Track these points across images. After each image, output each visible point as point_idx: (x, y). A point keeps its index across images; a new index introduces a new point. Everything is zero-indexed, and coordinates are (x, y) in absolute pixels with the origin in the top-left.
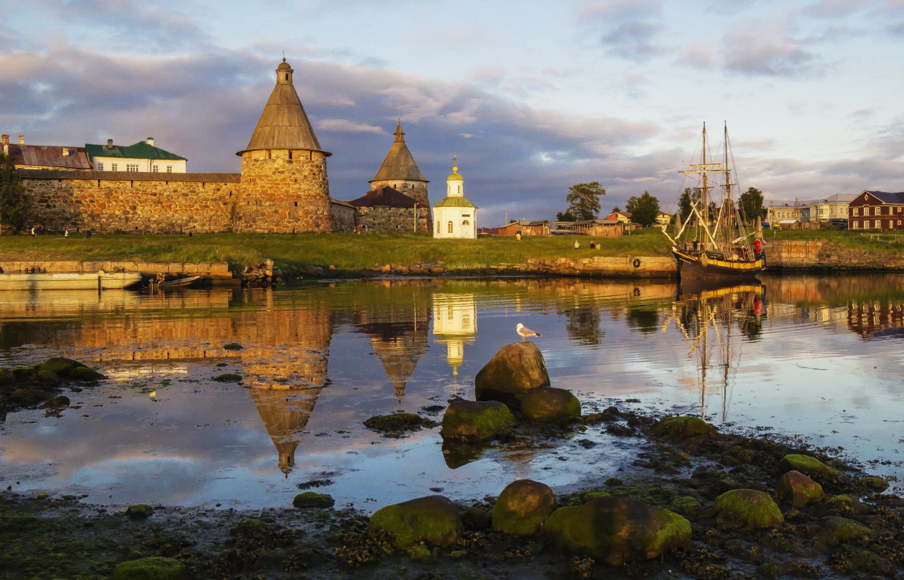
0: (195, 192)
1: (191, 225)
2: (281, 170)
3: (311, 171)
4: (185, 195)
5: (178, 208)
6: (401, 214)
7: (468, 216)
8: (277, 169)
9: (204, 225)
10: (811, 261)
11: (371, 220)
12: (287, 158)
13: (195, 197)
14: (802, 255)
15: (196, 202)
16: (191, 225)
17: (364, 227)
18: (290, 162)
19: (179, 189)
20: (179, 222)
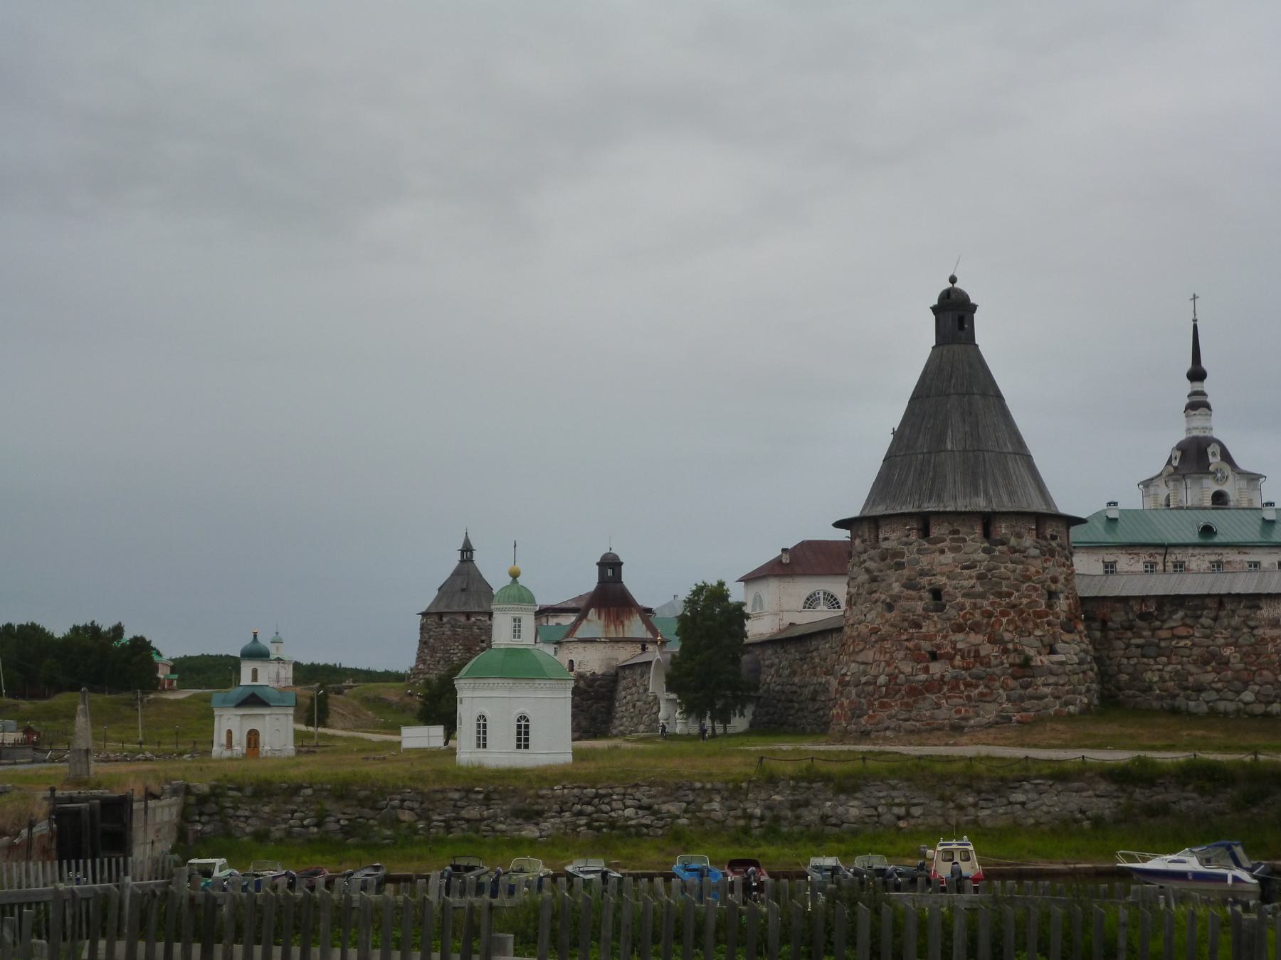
3: (868, 570)
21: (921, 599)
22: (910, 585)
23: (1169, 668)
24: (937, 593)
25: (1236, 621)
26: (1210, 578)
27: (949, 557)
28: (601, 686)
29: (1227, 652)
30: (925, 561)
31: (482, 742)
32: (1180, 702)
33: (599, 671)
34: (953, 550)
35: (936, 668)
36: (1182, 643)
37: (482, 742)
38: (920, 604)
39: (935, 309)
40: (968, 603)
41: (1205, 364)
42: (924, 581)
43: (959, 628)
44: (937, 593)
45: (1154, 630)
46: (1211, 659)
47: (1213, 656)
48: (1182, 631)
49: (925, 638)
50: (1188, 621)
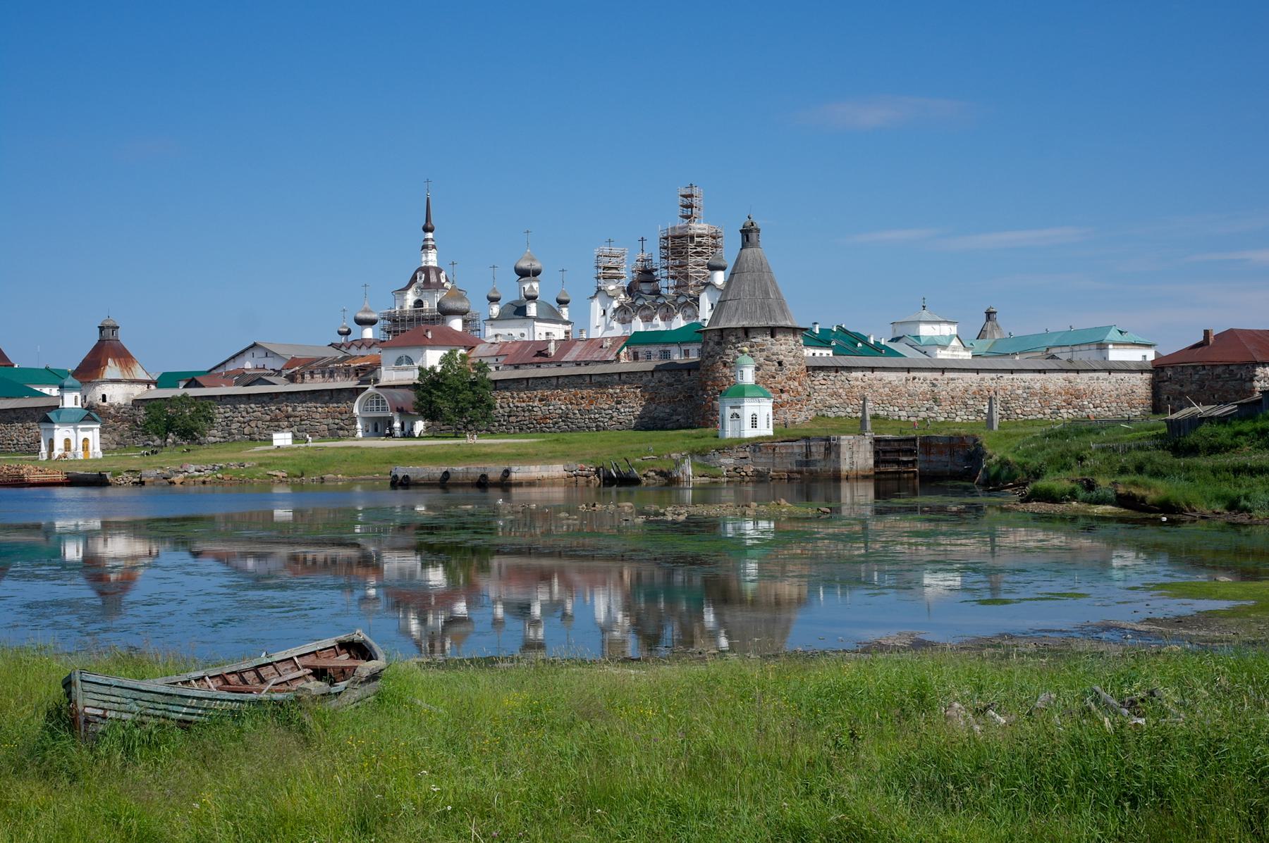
0: (680, 381)
1: (675, 418)
2: (711, 353)
4: (670, 385)
5: (662, 400)
6: (1218, 376)
7: (739, 407)
8: (709, 353)
9: (688, 418)
10: (958, 466)
11: (1178, 387)
12: (716, 339)
13: (679, 387)
14: (944, 458)
15: (680, 393)
16: (675, 418)
17: (1168, 398)
18: (719, 344)
19: (664, 379)
20: (662, 415)
21: (774, 365)
22: (768, 359)
23: (819, 398)
24: (780, 363)
25: (843, 378)
26: (1044, 361)
27: (783, 347)
28: (124, 413)
29: (841, 391)
30: (775, 349)
31: (754, 425)
32: (825, 412)
33: (122, 403)
34: (786, 344)
35: (785, 396)
36: (824, 387)
37: (754, 425)
38: (774, 368)
39: (741, 231)
40: (791, 367)
41: (434, 221)
42: (774, 357)
43: (790, 379)
44: (780, 363)
45: (812, 381)
46: (835, 394)
47: (835, 392)
48: (823, 382)
49: (780, 383)
50: (825, 377)
